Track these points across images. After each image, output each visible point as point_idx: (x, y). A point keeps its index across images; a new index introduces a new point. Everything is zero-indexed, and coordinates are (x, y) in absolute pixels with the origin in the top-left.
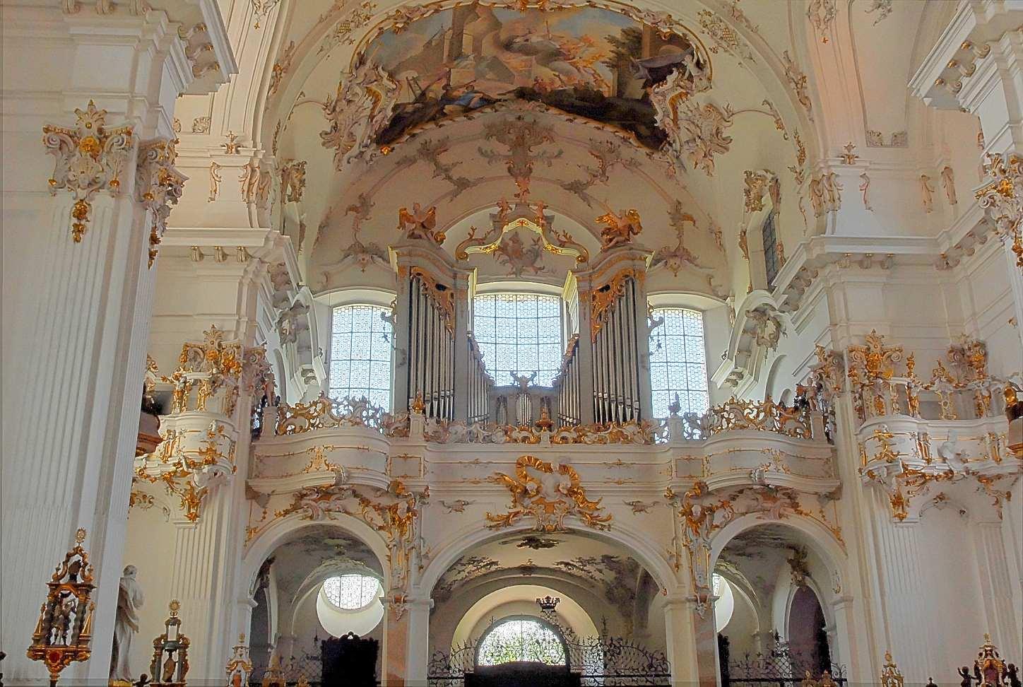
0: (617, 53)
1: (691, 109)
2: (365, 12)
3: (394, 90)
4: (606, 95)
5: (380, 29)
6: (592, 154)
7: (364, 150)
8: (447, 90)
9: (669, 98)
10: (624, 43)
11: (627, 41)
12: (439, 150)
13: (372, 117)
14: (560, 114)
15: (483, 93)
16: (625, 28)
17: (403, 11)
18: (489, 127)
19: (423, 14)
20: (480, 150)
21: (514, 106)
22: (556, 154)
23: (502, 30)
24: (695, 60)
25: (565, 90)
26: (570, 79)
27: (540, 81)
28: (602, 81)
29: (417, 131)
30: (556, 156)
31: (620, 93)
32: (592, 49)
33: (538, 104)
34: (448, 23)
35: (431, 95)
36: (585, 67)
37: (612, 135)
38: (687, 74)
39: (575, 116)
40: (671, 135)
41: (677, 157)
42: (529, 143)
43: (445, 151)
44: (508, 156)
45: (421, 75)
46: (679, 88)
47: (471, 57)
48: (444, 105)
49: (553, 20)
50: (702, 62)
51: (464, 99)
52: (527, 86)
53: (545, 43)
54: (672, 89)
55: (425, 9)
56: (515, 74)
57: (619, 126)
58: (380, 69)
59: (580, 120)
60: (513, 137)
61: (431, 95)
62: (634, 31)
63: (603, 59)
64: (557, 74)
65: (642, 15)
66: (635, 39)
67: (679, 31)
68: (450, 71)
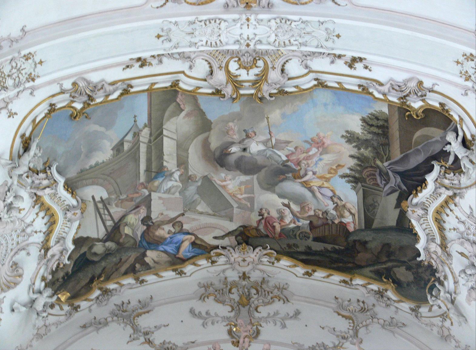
0: (358, 158)
1: (463, 218)
2: (28, 67)
3: (74, 207)
4: (351, 228)
5: (51, 105)
6: (339, 314)
7: (35, 296)
8: (149, 227)
9: (431, 210)
10: (366, 140)
11: (369, 136)
12: (140, 311)
13: (45, 247)
14: (295, 266)
15: (197, 238)
16: (365, 116)
17: (82, 84)
18: (204, 286)
19: (109, 95)
20: (192, 311)
21: (236, 256)
22: (291, 315)
23: (212, 132)
24: (460, 139)
25: (298, 227)
26: (303, 208)
27: (266, 215)
28: (344, 206)
29: (111, 286)
30: (291, 317)
31: (368, 222)
32: (327, 158)
33: (265, 252)
34: (143, 119)
35: (127, 230)
36: (320, 187)
37: (363, 290)
38: (451, 159)
39: (314, 268)
40: (440, 268)
41: (453, 302)
42: (256, 302)
43: (148, 312)
44: (228, 318)
45: (113, 197)
46: (443, 190)
47: (177, 175)
48: (146, 250)
49: (275, 115)
50: (469, 137)
51: (170, 243)
52: (249, 224)
53: (269, 153)
54: (436, 194)
55: (112, 88)
56: (235, 205)
57: (372, 275)
58: (54, 169)
59: (320, 274)
60: (235, 296)
61: (127, 230)
62: (377, 119)
63: (341, 172)
64: (286, 201)
65: (385, 89)
66: (380, 131)
67: (434, 102)
68: (150, 195)
